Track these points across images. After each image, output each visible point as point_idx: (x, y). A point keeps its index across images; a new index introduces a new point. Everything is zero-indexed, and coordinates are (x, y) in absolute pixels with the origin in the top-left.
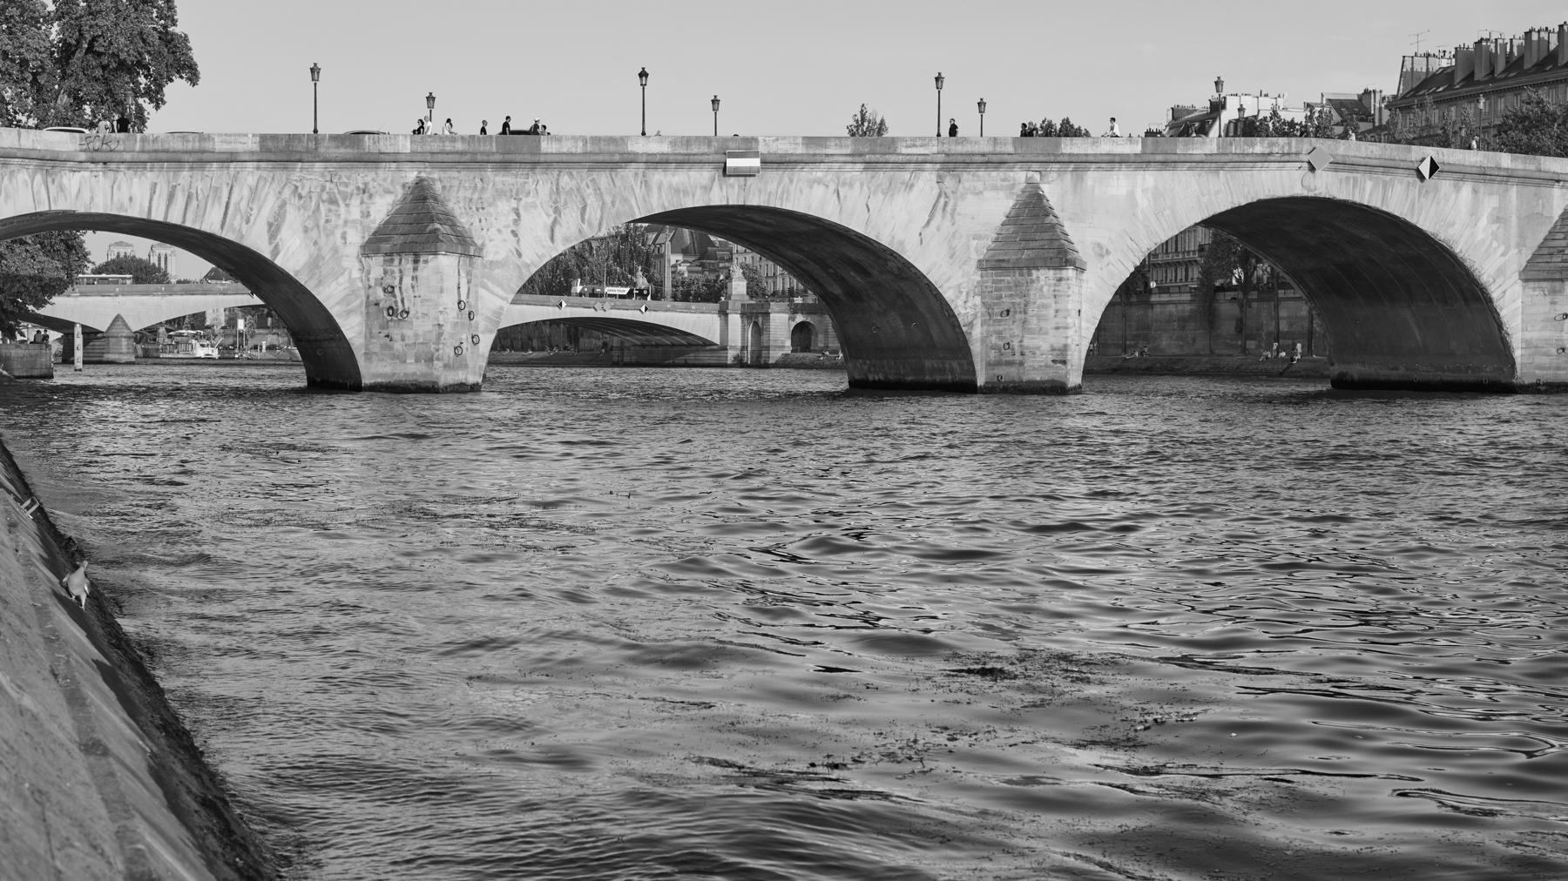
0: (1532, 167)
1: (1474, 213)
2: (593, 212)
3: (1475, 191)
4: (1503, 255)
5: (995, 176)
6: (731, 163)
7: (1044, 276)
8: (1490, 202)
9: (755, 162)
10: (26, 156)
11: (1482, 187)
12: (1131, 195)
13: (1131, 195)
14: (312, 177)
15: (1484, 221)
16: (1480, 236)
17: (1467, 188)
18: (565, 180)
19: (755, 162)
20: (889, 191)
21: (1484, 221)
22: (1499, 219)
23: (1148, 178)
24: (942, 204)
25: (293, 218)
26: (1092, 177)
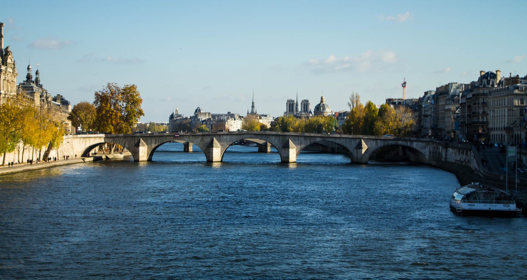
1: (275, 139)
2: (160, 142)
3: (275, 137)
5: (209, 137)
6: (176, 136)
7: (211, 148)
8: (277, 138)
9: (178, 136)
10: (97, 137)
12: (227, 138)
13: (227, 138)
14: (129, 139)
15: (276, 141)
18: (157, 138)
19: (178, 136)
20: (195, 139)
21: (276, 141)
22: (279, 140)
23: (229, 136)
24: (202, 140)
25: (127, 143)
26: (221, 137)
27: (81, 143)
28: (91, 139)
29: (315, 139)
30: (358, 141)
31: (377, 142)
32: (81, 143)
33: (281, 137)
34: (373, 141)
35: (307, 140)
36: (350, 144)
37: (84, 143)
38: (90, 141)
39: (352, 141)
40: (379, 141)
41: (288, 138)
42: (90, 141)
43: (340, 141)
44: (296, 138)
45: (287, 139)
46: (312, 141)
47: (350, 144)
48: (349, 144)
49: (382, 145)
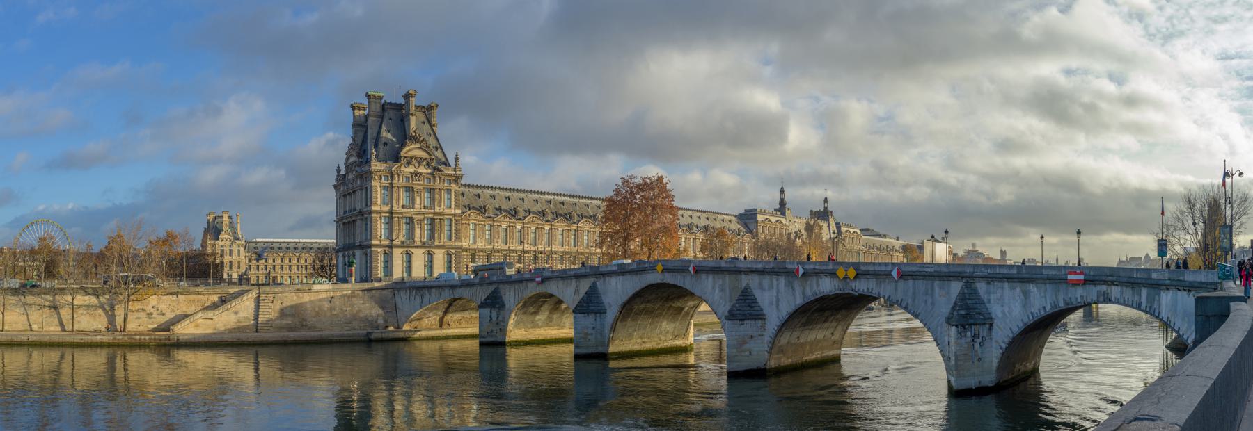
0: (732, 266)
1: (713, 288)
3: (714, 278)
4: (724, 306)
11: (716, 276)
15: (717, 291)
16: (716, 298)
17: (711, 277)
21: (717, 291)
27: (412, 298)
28: (433, 290)
29: (818, 285)
30: (956, 287)
31: (1026, 294)
32: (412, 298)
33: (727, 278)
34: (1013, 288)
35: (793, 289)
36: (930, 301)
37: (418, 298)
38: (430, 294)
39: (937, 290)
40: (1032, 287)
41: (744, 280)
42: (430, 294)
43: (896, 289)
44: (766, 280)
45: (744, 285)
46: (809, 292)
47: (930, 301)
48: (926, 301)
49: (1048, 308)
